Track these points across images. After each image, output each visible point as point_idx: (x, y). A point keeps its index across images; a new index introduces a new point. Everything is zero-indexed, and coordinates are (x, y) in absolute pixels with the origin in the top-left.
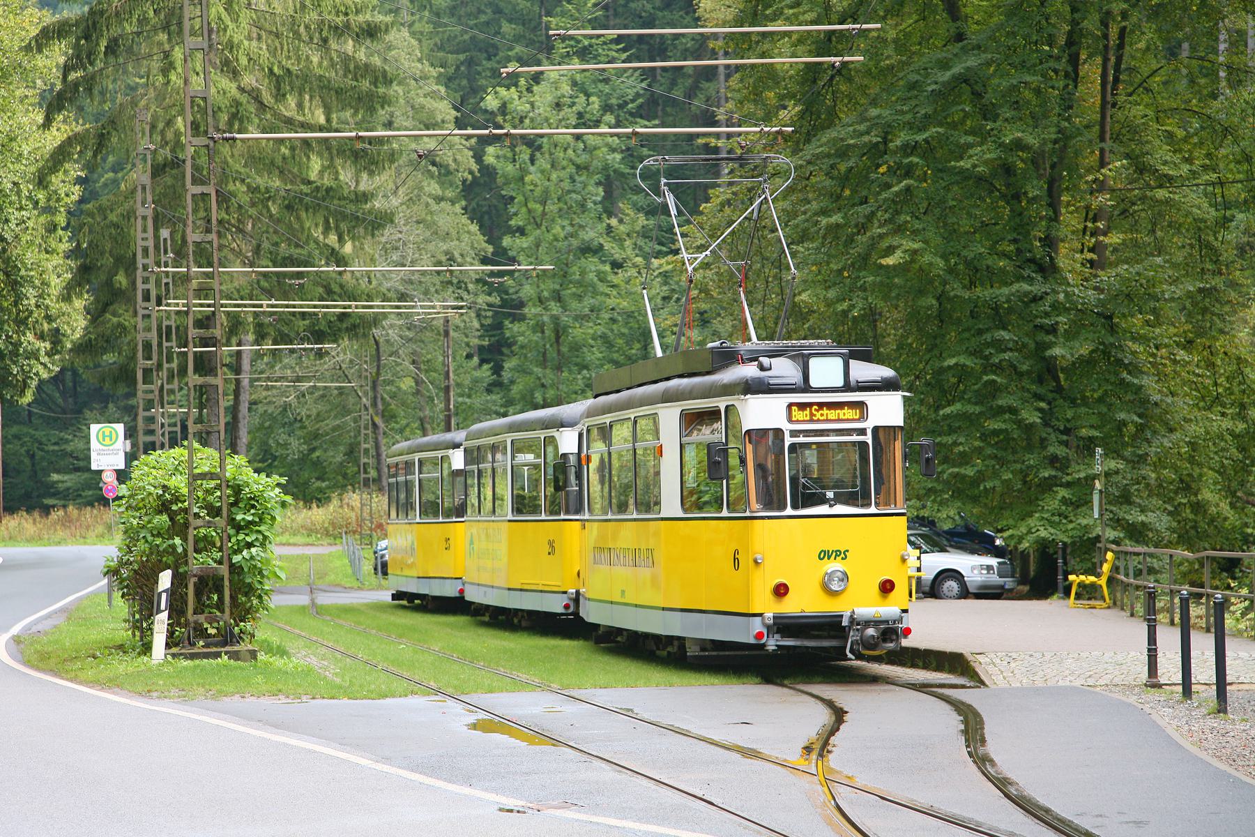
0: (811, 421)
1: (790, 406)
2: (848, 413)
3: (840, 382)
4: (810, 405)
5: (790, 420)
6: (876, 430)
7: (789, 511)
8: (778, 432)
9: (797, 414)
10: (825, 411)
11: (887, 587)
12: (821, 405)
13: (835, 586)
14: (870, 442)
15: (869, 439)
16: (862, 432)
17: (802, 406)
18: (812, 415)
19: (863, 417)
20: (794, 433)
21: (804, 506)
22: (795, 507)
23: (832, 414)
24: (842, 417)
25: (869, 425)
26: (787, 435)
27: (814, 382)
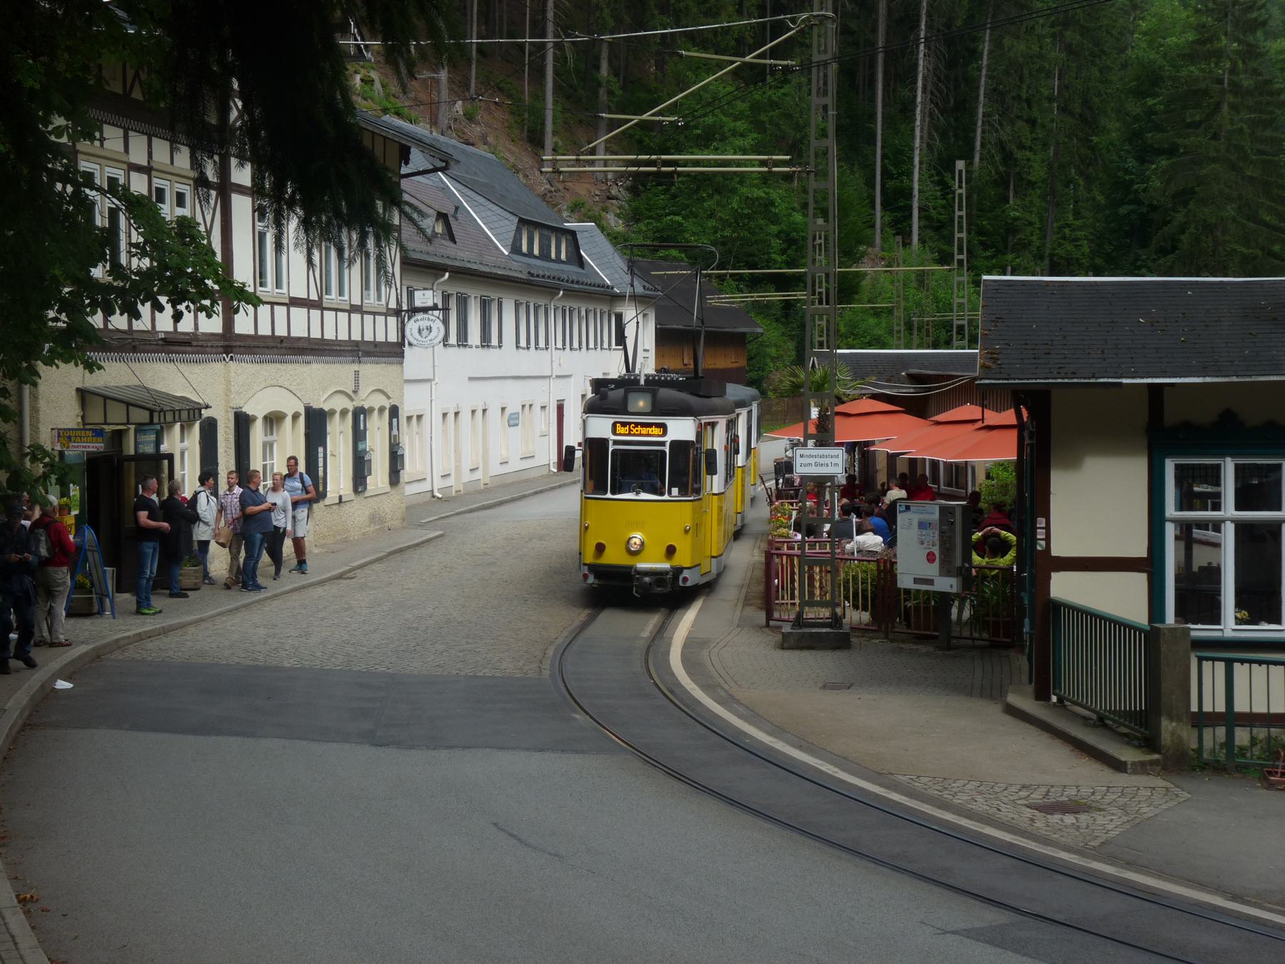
0: (629, 434)
1: (614, 425)
2: (656, 431)
4: (630, 424)
5: (614, 433)
6: (673, 443)
8: (604, 442)
9: (620, 429)
11: (671, 551)
12: (637, 424)
16: (663, 444)
17: (624, 424)
19: (665, 433)
20: (615, 442)
22: (613, 493)
23: (644, 431)
25: (668, 439)
27: (630, 409)
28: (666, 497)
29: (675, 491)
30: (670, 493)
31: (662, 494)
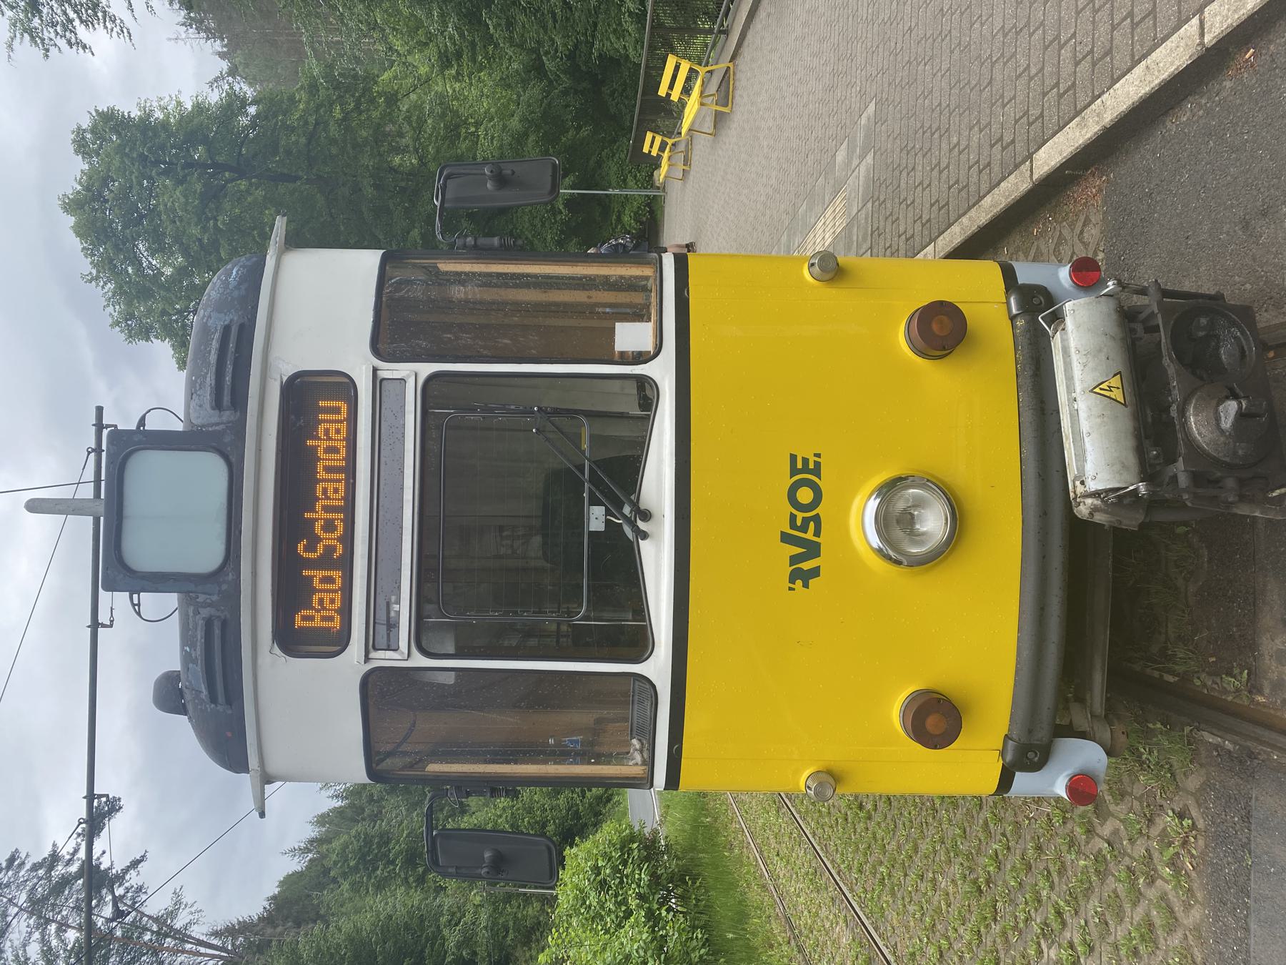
0: (346, 564)
1: (292, 641)
2: (328, 432)
3: (208, 471)
7: (657, 668)
8: (380, 691)
10: (318, 515)
13: (933, 523)
14: (427, 369)
15: (413, 373)
17: (291, 591)
18: (326, 561)
19: (343, 386)
21: (640, 608)
22: (639, 645)
23: (328, 489)
24: (338, 460)
26: (384, 659)
28: (662, 372)
29: (631, 336)
30: (641, 358)
31: (645, 391)
